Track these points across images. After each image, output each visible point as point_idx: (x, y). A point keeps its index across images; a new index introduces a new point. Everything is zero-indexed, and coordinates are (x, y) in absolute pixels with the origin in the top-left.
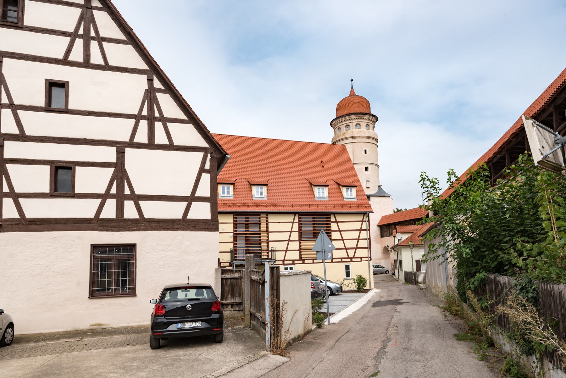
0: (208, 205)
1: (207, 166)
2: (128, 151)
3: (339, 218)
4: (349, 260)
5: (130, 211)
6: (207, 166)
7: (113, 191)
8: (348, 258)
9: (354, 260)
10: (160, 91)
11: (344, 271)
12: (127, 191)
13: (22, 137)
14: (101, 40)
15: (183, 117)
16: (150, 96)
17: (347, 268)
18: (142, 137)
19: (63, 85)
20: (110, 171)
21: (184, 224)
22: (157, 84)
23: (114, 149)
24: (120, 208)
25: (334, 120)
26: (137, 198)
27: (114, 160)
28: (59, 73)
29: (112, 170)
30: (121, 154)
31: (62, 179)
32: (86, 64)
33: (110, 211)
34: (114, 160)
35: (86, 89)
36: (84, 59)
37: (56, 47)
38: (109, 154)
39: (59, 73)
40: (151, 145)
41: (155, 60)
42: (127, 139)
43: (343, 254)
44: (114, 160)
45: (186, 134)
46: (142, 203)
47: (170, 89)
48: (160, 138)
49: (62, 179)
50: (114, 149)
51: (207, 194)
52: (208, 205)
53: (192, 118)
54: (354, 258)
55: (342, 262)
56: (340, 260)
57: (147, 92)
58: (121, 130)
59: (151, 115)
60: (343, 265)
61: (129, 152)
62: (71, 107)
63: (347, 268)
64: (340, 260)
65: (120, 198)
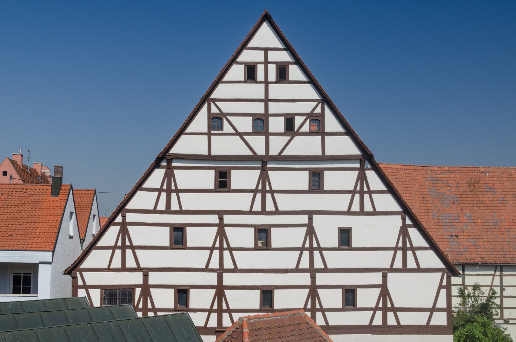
2: (390, 275)
5: (391, 321)
7: (380, 305)
12: (389, 305)
18: (398, 264)
20: (379, 290)
23: (380, 274)
24: (385, 318)
26: (395, 310)
27: (380, 282)
29: (379, 290)
30: (385, 277)
34: (380, 282)
35: (363, 231)
42: (388, 266)
46: (399, 314)
48: (411, 264)
50: (380, 274)
58: (383, 260)
59: (404, 246)
61: (390, 275)
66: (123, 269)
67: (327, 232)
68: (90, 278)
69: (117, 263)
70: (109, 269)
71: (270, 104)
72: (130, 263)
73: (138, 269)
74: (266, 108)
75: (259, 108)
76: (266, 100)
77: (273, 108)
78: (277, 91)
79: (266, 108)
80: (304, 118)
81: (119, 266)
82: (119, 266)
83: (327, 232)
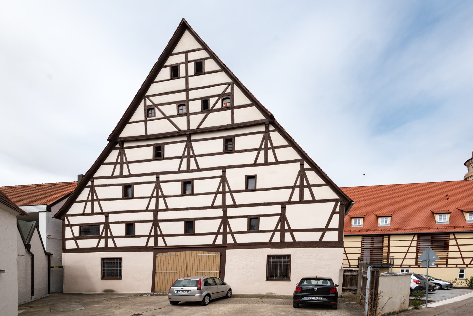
0: (337, 233)
1: (338, 210)
3: (457, 236)
4: (465, 266)
6: (338, 210)
8: (464, 264)
9: (469, 266)
10: (308, 170)
11: (459, 273)
13: (235, 206)
14: (273, 148)
15: (323, 182)
16: (302, 174)
17: (462, 271)
19: (254, 177)
21: (321, 244)
22: (306, 166)
25: (469, 160)
28: (251, 171)
31: (253, 224)
32: (266, 163)
33: (277, 238)
36: (265, 161)
37: (250, 158)
38: (277, 209)
39: (251, 171)
40: (301, 201)
41: (306, 152)
43: (460, 261)
44: (280, 212)
45: (325, 192)
47: (314, 167)
49: (253, 224)
51: (337, 226)
52: (337, 233)
53: (328, 182)
54: (470, 264)
55: (456, 267)
56: (455, 266)
57: (300, 171)
60: (458, 270)
62: (258, 187)
63: (462, 271)
64: (455, 266)
65: (283, 232)
66: (93, 213)
67: (236, 179)
68: (73, 220)
69: (88, 210)
70: (84, 214)
71: (190, 92)
72: (97, 210)
73: (102, 213)
74: (187, 96)
75: (182, 97)
76: (187, 90)
77: (192, 94)
78: (195, 81)
79: (187, 96)
80: (216, 99)
81: (90, 212)
82: (90, 212)
83: (236, 179)
